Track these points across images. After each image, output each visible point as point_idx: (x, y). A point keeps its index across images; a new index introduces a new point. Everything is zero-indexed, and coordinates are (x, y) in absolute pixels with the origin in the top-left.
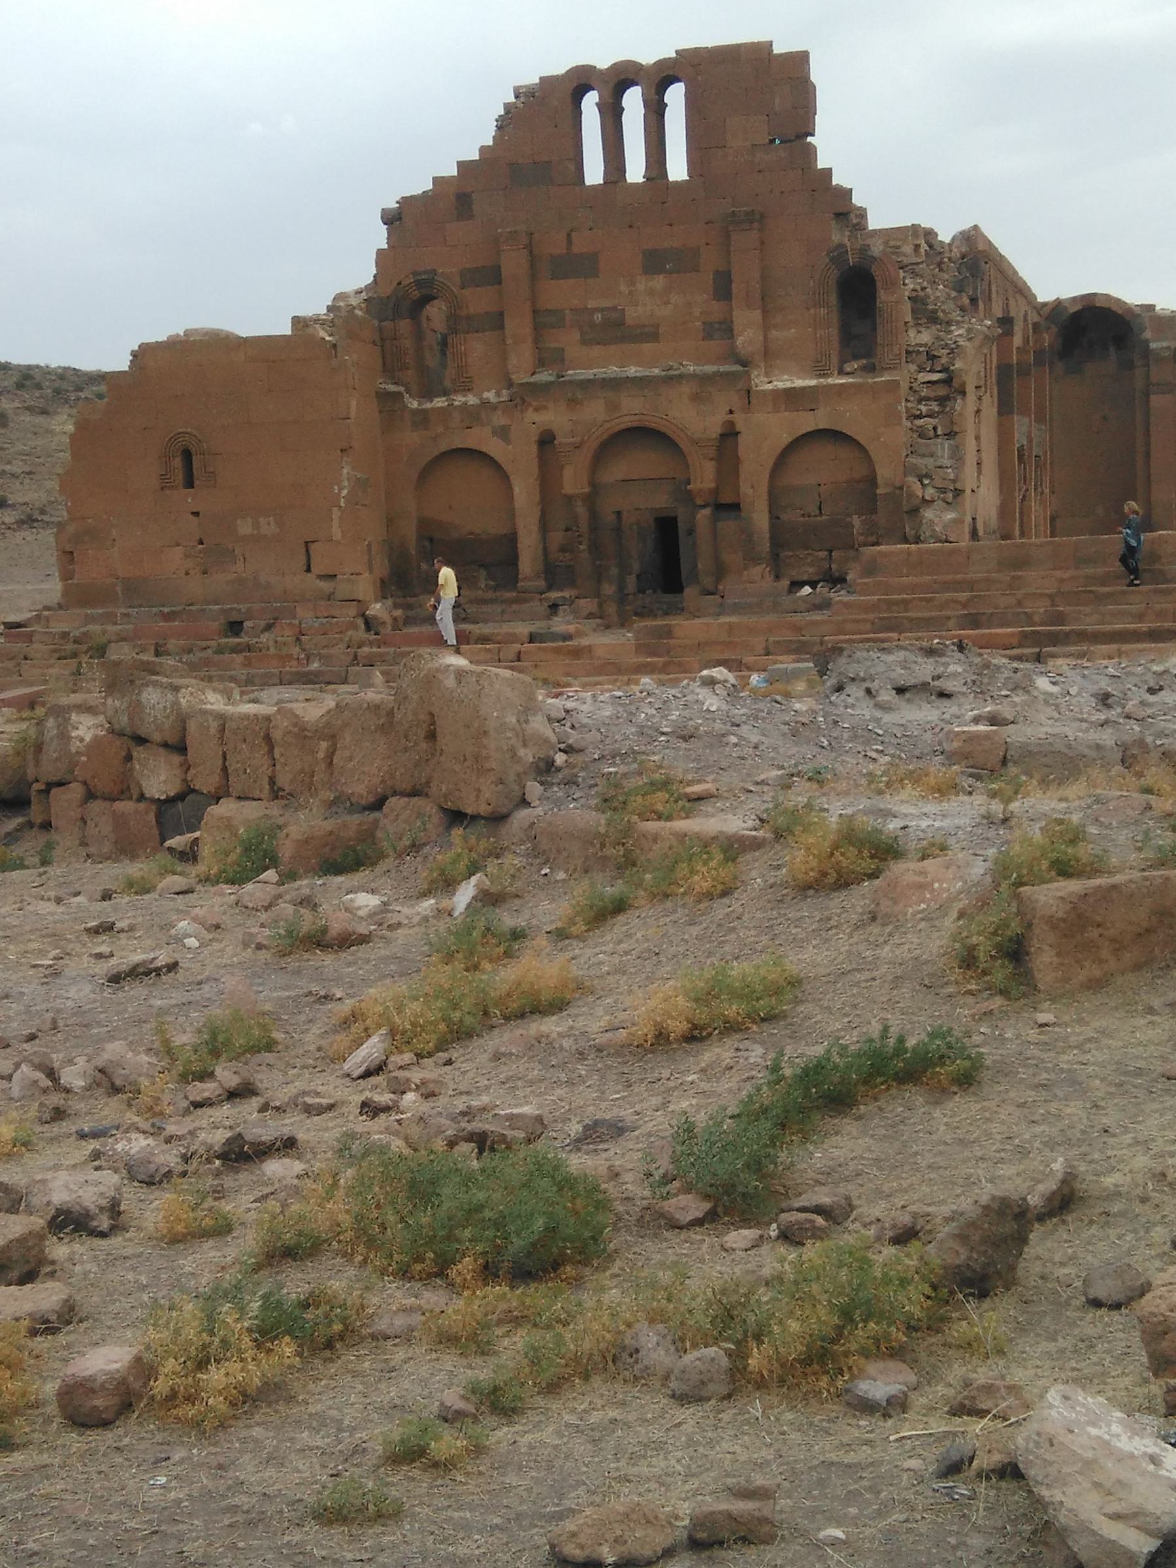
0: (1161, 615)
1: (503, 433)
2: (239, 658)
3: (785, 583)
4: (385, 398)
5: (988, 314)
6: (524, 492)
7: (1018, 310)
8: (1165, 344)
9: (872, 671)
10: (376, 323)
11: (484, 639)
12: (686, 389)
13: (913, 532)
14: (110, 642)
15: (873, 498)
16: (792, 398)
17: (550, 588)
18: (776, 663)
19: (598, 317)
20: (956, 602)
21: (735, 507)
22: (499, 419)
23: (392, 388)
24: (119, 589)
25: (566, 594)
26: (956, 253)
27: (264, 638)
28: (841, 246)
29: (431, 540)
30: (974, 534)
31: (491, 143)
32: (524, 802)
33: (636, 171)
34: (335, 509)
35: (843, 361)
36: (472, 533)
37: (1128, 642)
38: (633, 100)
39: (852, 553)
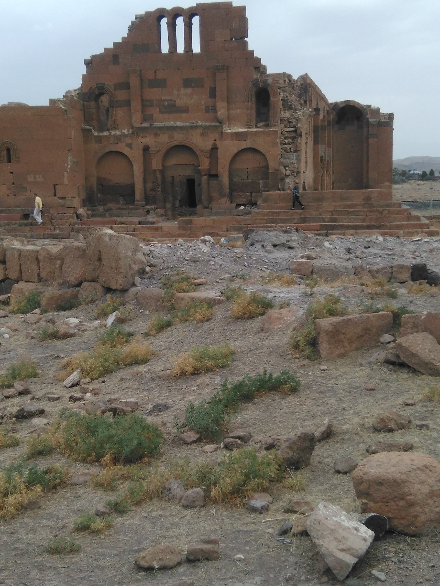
0: (371, 219)
2: (28, 228)
3: (234, 205)
5: (310, 106)
7: (321, 106)
8: (375, 120)
9: (264, 238)
10: (82, 102)
11: (122, 223)
12: (199, 131)
13: (282, 187)
15: (267, 173)
16: (238, 135)
18: (231, 234)
19: (166, 103)
20: (297, 213)
21: (216, 176)
22: (128, 140)
23: (88, 127)
26: (299, 84)
28: (257, 79)
29: (102, 185)
30: (304, 188)
31: (126, 36)
32: (134, 285)
33: (181, 48)
34: (66, 173)
35: (257, 122)
36: (118, 183)
37: (358, 229)
38: (180, 22)
39: (259, 194)
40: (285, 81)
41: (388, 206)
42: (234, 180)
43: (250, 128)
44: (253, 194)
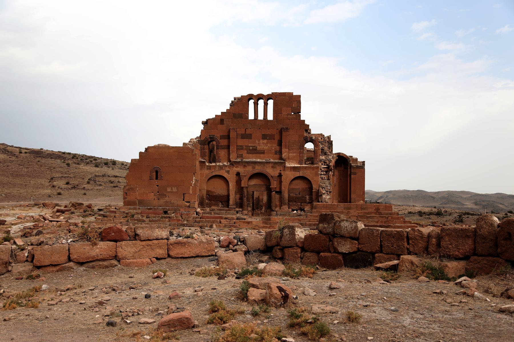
1: (228, 172)
4: (201, 162)
6: (232, 185)
12: (271, 165)
14: (135, 214)
15: (312, 192)
16: (294, 169)
17: (236, 207)
19: (251, 148)
22: (227, 169)
24: (137, 202)
25: (240, 209)
27: (173, 215)
33: (261, 117)
40: (322, 138)
41: (390, 214)
42: (291, 195)
43: (302, 164)
44: (302, 204)
